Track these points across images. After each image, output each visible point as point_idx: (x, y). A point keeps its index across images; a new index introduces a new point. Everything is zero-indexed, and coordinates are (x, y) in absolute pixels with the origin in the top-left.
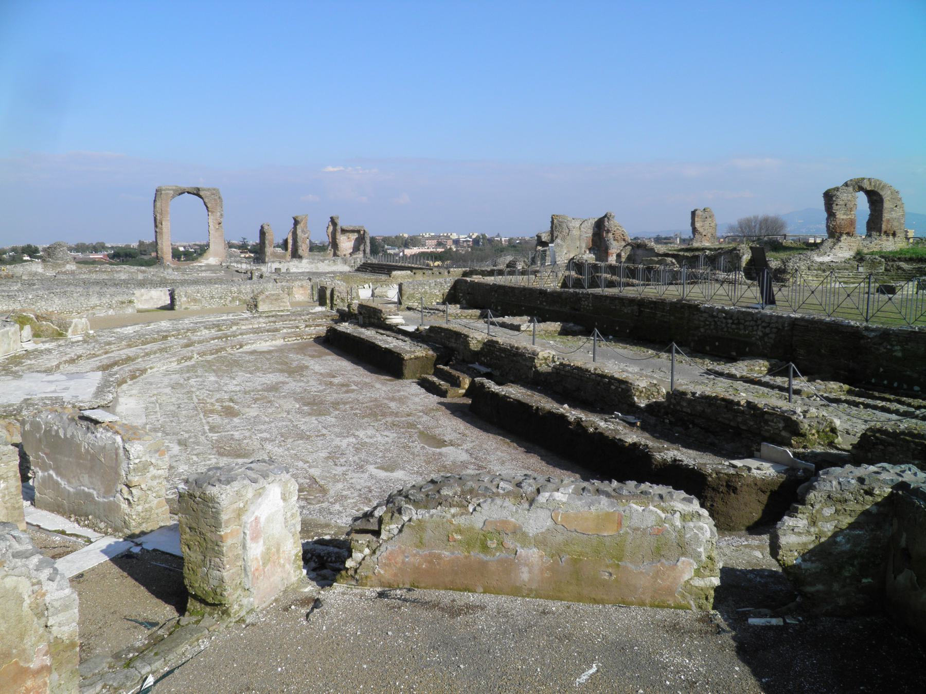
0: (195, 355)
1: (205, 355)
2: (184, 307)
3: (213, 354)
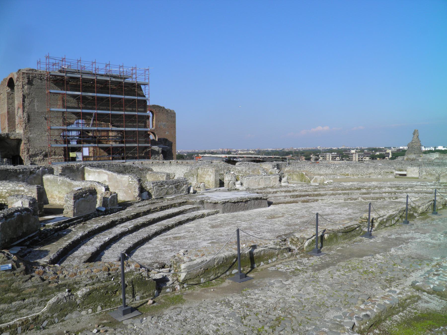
0: (360, 198)
1: (368, 199)
2: (424, 177)
3: (374, 199)
